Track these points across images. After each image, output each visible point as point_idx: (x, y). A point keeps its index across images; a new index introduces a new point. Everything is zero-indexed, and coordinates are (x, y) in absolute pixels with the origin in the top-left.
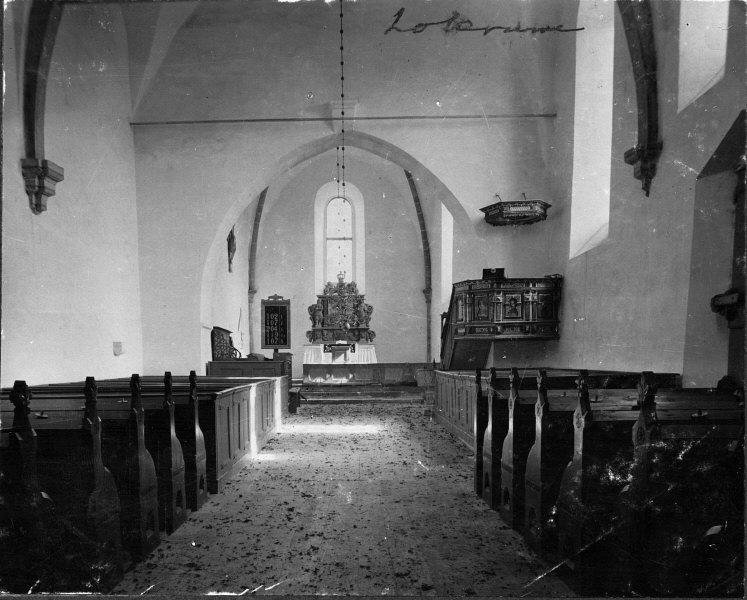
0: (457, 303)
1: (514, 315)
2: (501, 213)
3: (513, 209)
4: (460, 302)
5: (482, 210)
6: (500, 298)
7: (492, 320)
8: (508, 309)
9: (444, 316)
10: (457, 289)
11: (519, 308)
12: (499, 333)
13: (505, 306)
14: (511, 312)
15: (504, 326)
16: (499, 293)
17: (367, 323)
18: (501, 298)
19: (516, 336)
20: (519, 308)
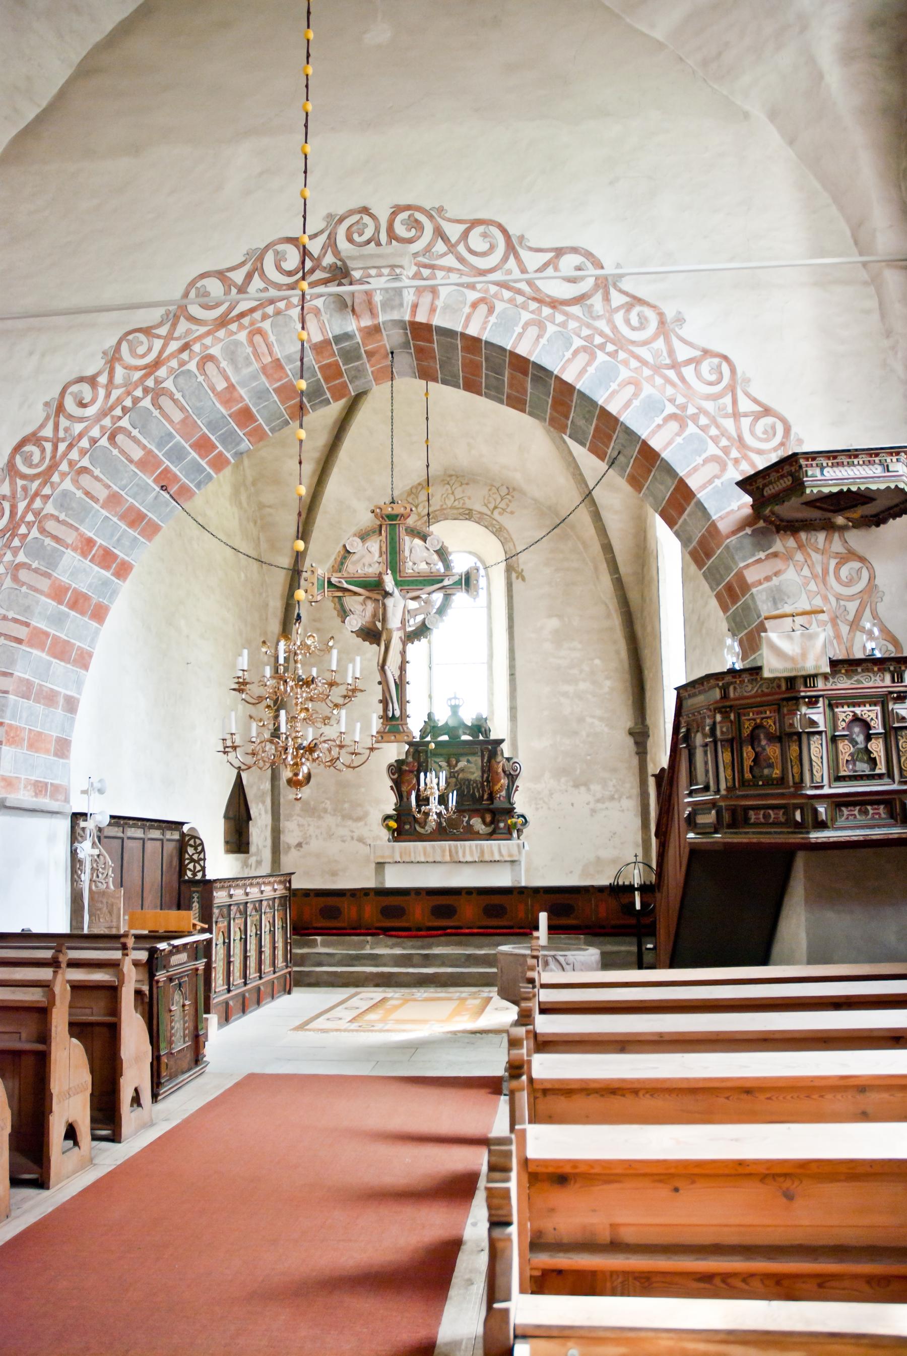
0: (687, 738)
1: (863, 767)
2: (798, 486)
3: (829, 473)
4: (699, 739)
5: (746, 484)
6: (818, 715)
7: (799, 784)
8: (845, 749)
9: (659, 778)
10: (689, 703)
11: (877, 748)
12: (822, 825)
13: (834, 739)
14: (853, 759)
15: (839, 802)
16: (812, 702)
17: (509, 796)
18: (818, 715)
19: (877, 833)
20: (877, 748)
